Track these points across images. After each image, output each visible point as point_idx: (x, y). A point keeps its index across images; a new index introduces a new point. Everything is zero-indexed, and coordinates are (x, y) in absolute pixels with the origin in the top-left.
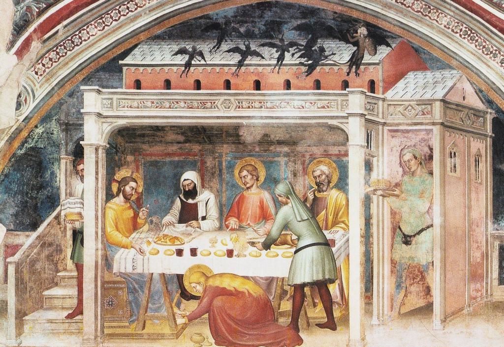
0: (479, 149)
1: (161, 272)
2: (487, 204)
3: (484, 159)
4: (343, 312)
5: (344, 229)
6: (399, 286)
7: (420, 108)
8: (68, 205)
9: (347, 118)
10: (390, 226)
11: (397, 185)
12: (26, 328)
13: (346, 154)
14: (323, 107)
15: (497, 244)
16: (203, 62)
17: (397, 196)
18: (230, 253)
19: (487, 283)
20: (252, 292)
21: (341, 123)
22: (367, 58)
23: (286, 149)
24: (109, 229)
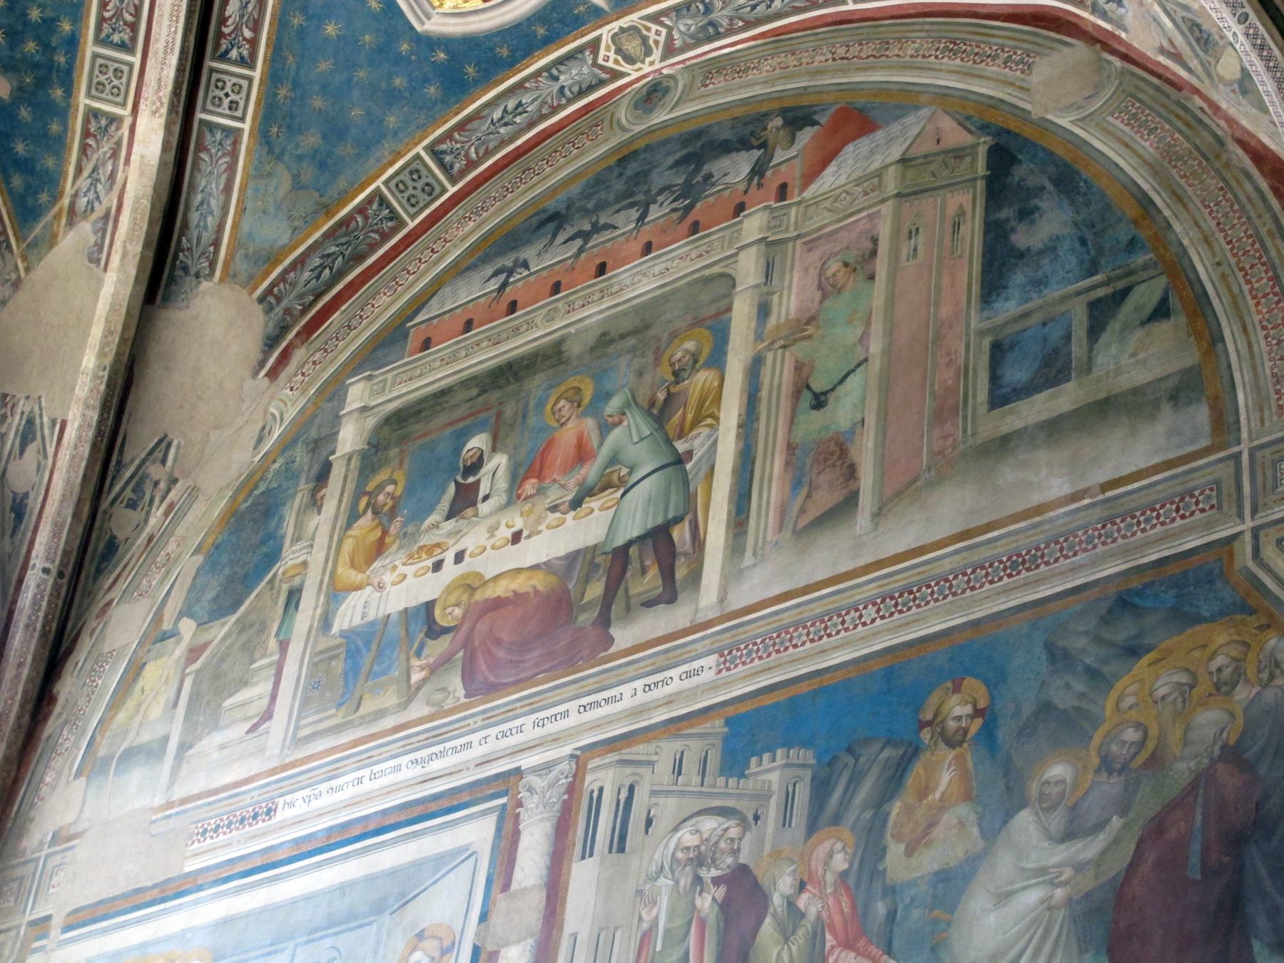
0: (961, 206)
1: (401, 607)
2: (970, 284)
3: (969, 216)
4: (693, 566)
5: (709, 426)
6: (796, 484)
7: (859, 189)
8: (291, 556)
9: (736, 255)
10: (791, 388)
11: (811, 320)
12: (185, 769)
13: (729, 309)
14: (701, 255)
15: (986, 343)
16: (526, 273)
17: (810, 337)
18: (516, 538)
19: (965, 417)
20: (540, 587)
21: (726, 266)
22: (779, 156)
23: (632, 341)
24: (340, 570)
